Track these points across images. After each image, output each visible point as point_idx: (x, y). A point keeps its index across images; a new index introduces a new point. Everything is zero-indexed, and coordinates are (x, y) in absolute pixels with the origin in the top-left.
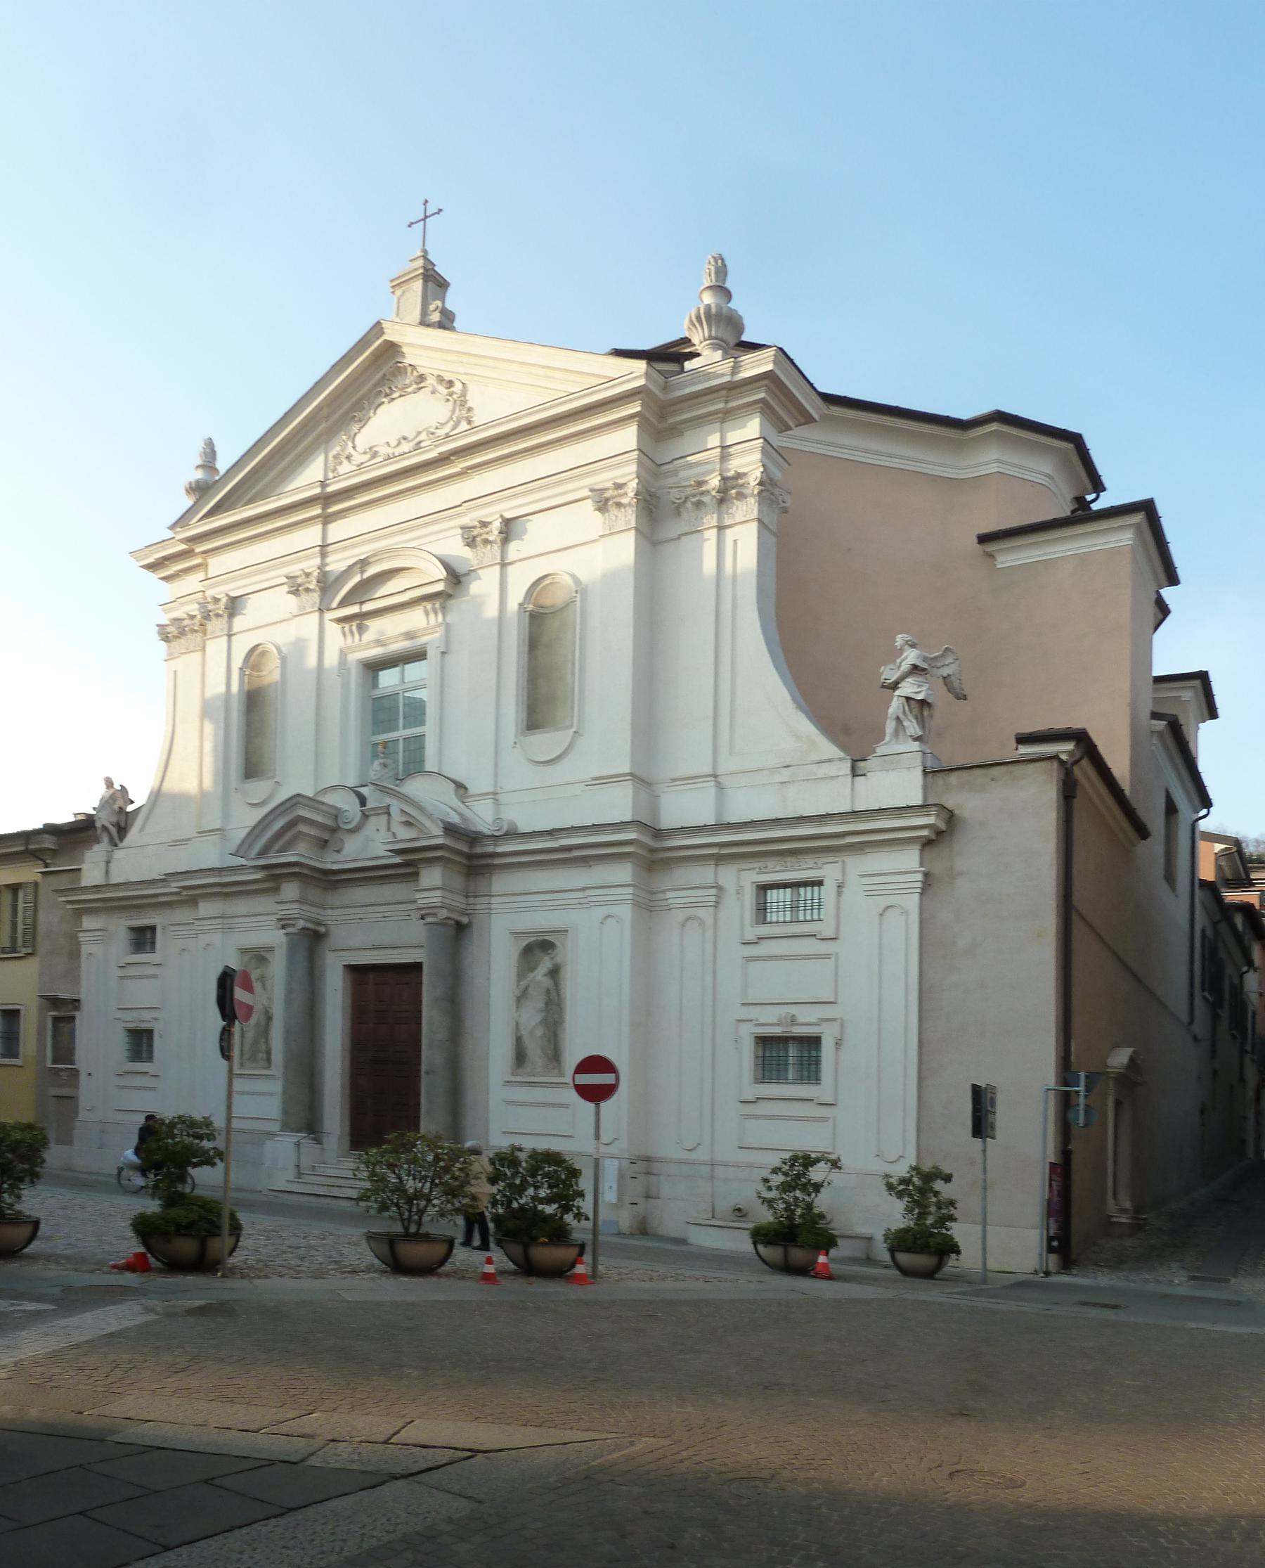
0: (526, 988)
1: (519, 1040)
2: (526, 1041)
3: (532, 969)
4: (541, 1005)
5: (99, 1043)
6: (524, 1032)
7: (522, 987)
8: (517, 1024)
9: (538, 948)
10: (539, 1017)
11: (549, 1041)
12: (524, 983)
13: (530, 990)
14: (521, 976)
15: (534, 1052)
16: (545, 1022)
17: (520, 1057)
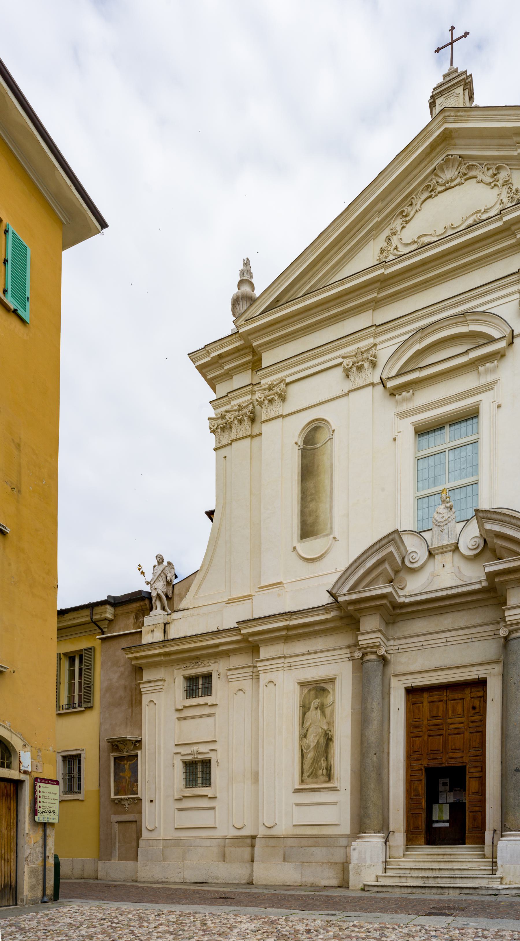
5: (159, 774)
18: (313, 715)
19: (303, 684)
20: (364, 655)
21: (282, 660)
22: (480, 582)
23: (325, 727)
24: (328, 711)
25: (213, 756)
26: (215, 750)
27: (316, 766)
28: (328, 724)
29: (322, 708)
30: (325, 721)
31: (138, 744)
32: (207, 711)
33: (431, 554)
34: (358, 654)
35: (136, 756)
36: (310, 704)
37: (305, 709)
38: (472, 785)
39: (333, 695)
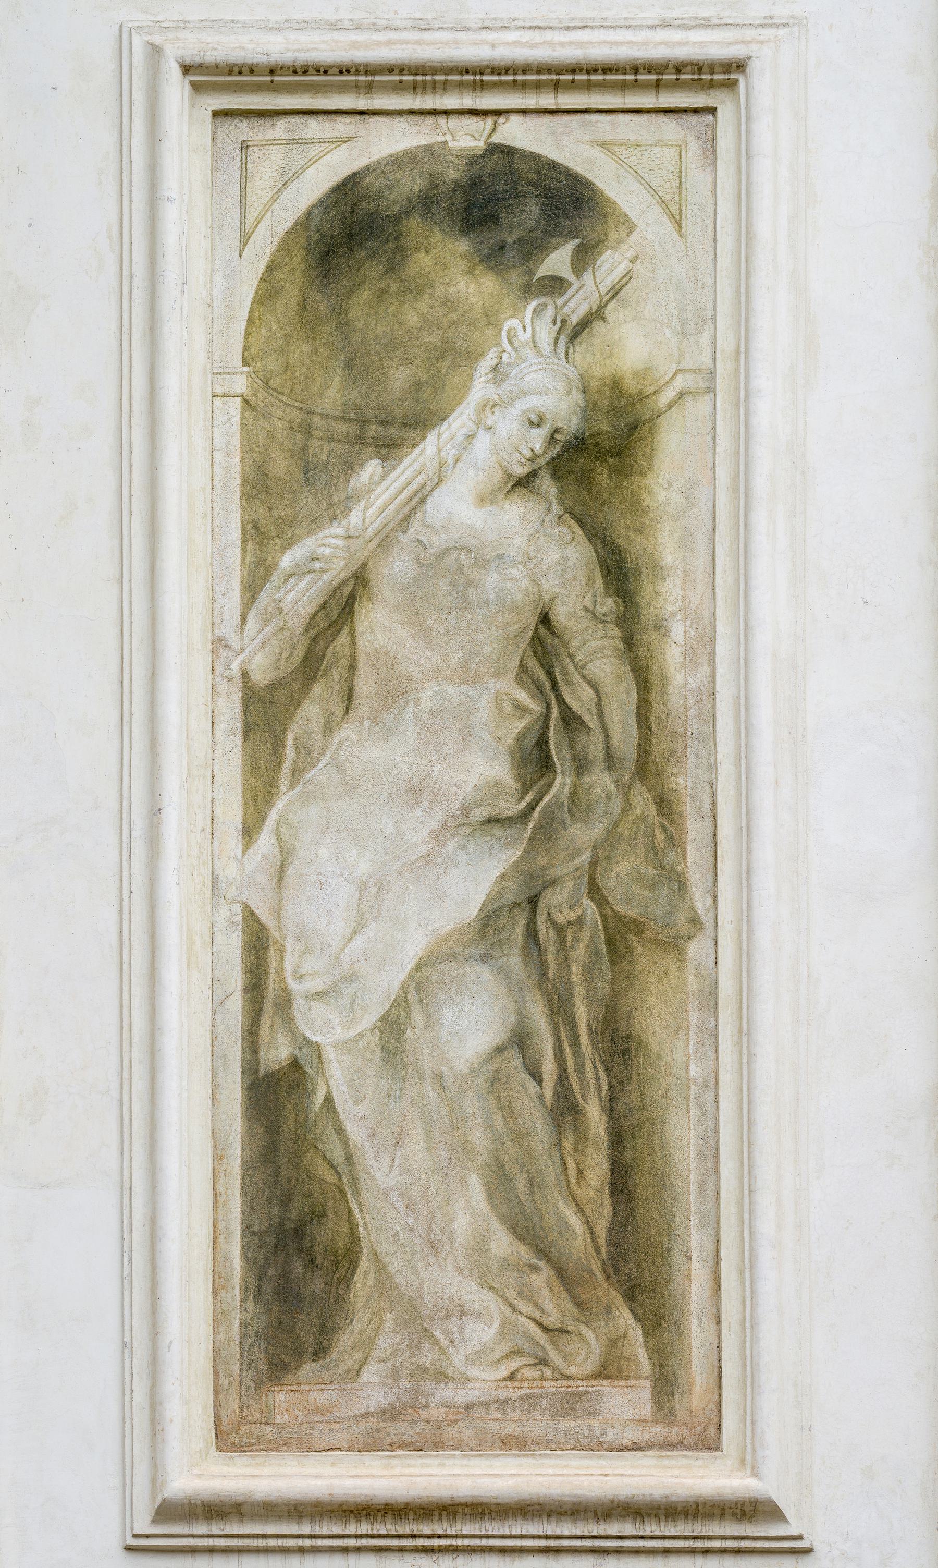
0: (341, 607)
1: (277, 1101)
3: (388, 429)
7: (298, 598)
8: (258, 944)
10: (476, 878)
11: (565, 1110)
12: (320, 553)
15: (427, 1207)
16: (518, 920)
17: (298, 1267)
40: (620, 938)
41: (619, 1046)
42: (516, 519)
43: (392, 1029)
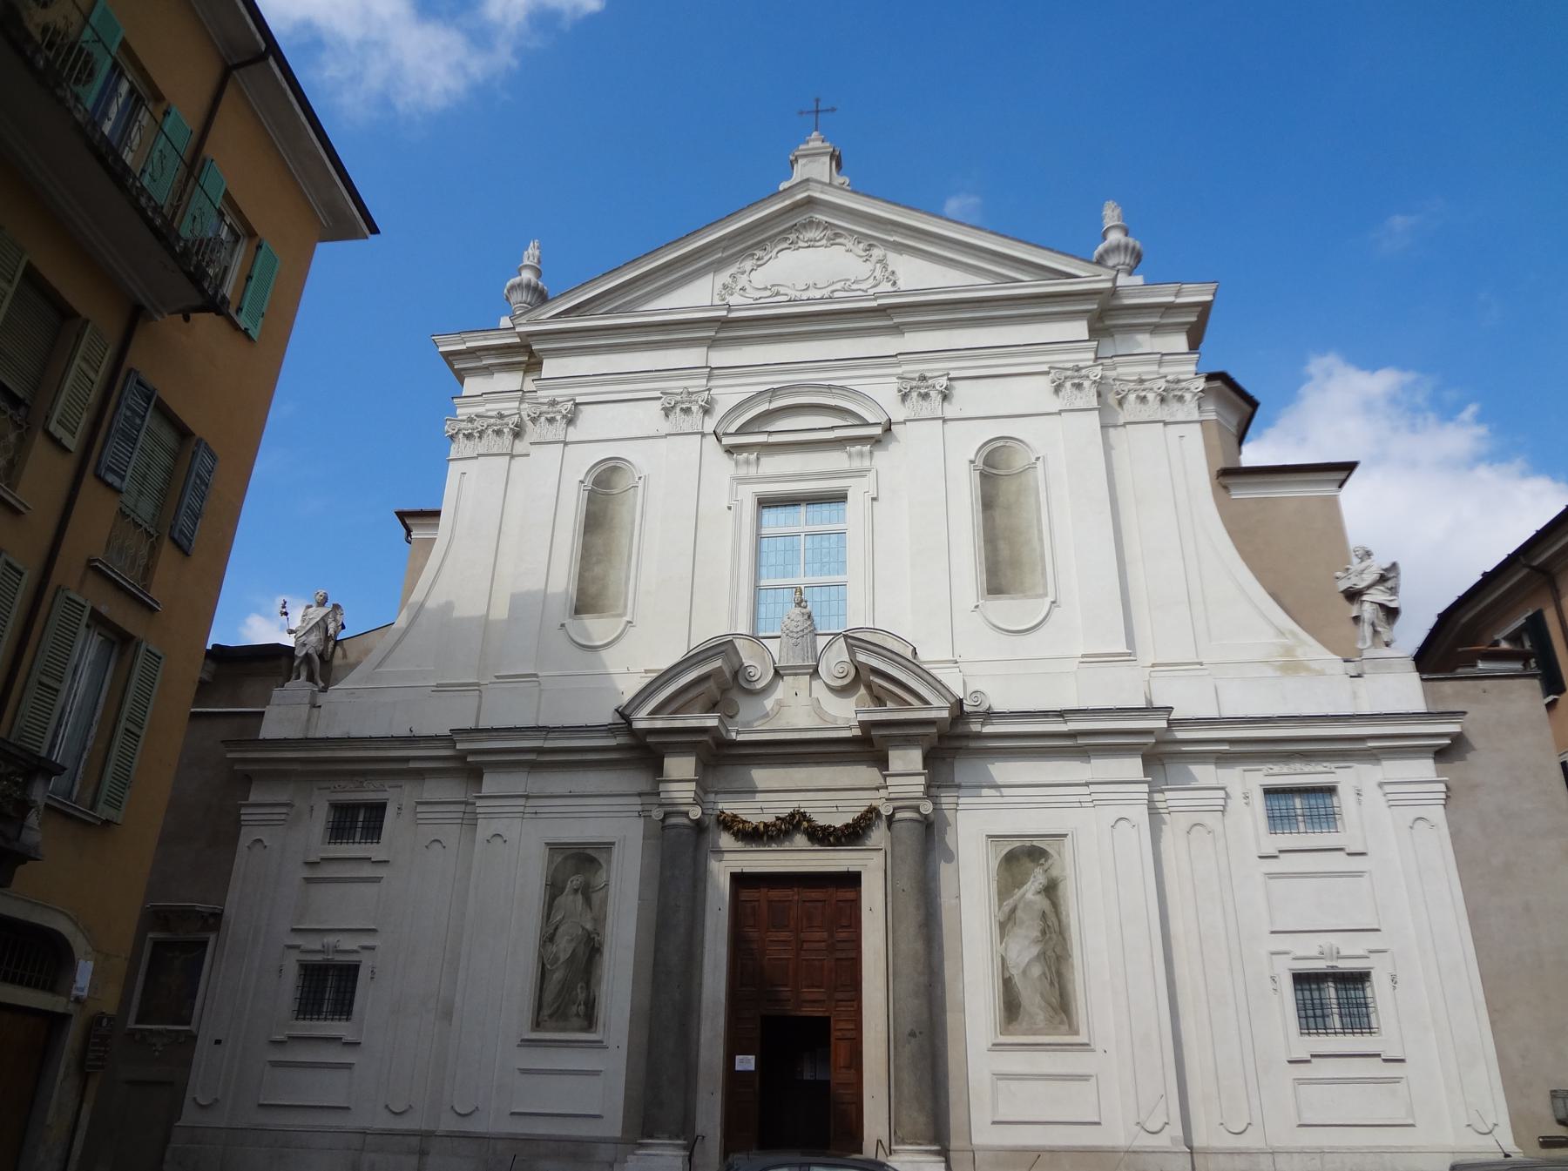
0: (1013, 910)
1: (1007, 983)
2: (1017, 980)
4: (1036, 933)
5: (246, 988)
6: (1014, 972)
7: (1006, 909)
8: (1003, 959)
9: (1023, 858)
10: (1035, 950)
11: (1052, 983)
13: (1019, 913)
14: (1004, 891)
16: (1042, 956)
17: (1011, 1007)
18: (570, 901)
19: (554, 847)
20: (667, 815)
21: (522, 802)
22: (850, 728)
23: (589, 926)
24: (596, 898)
25: (366, 961)
26: (372, 948)
27: (565, 996)
28: (595, 920)
29: (586, 891)
30: (589, 916)
31: (215, 920)
32: (367, 871)
33: (778, 673)
34: (657, 814)
35: (204, 944)
36: (565, 882)
37: (554, 889)
38: (840, 1052)
39: (608, 872)
40: (1058, 958)
41: (1059, 975)
42: (1038, 898)
43: (1024, 972)
